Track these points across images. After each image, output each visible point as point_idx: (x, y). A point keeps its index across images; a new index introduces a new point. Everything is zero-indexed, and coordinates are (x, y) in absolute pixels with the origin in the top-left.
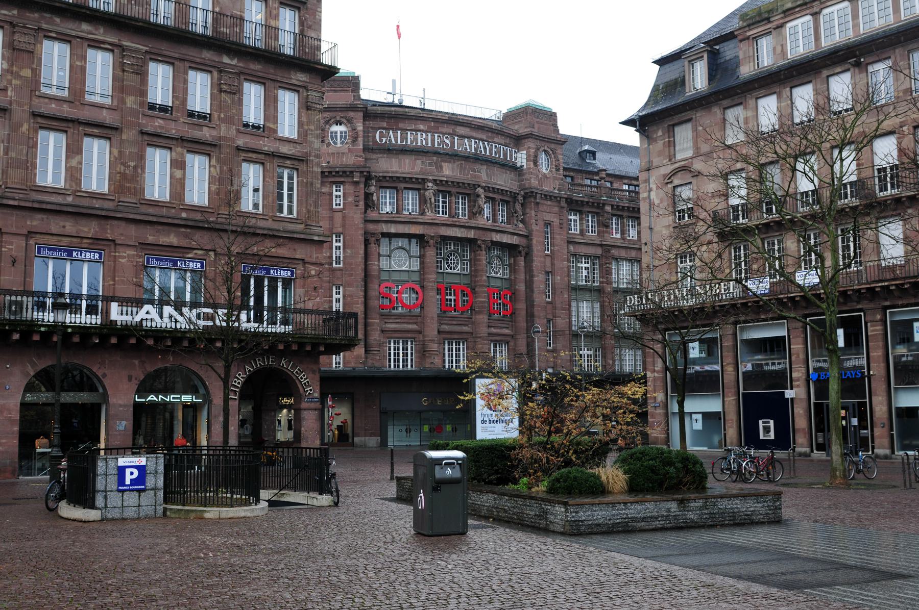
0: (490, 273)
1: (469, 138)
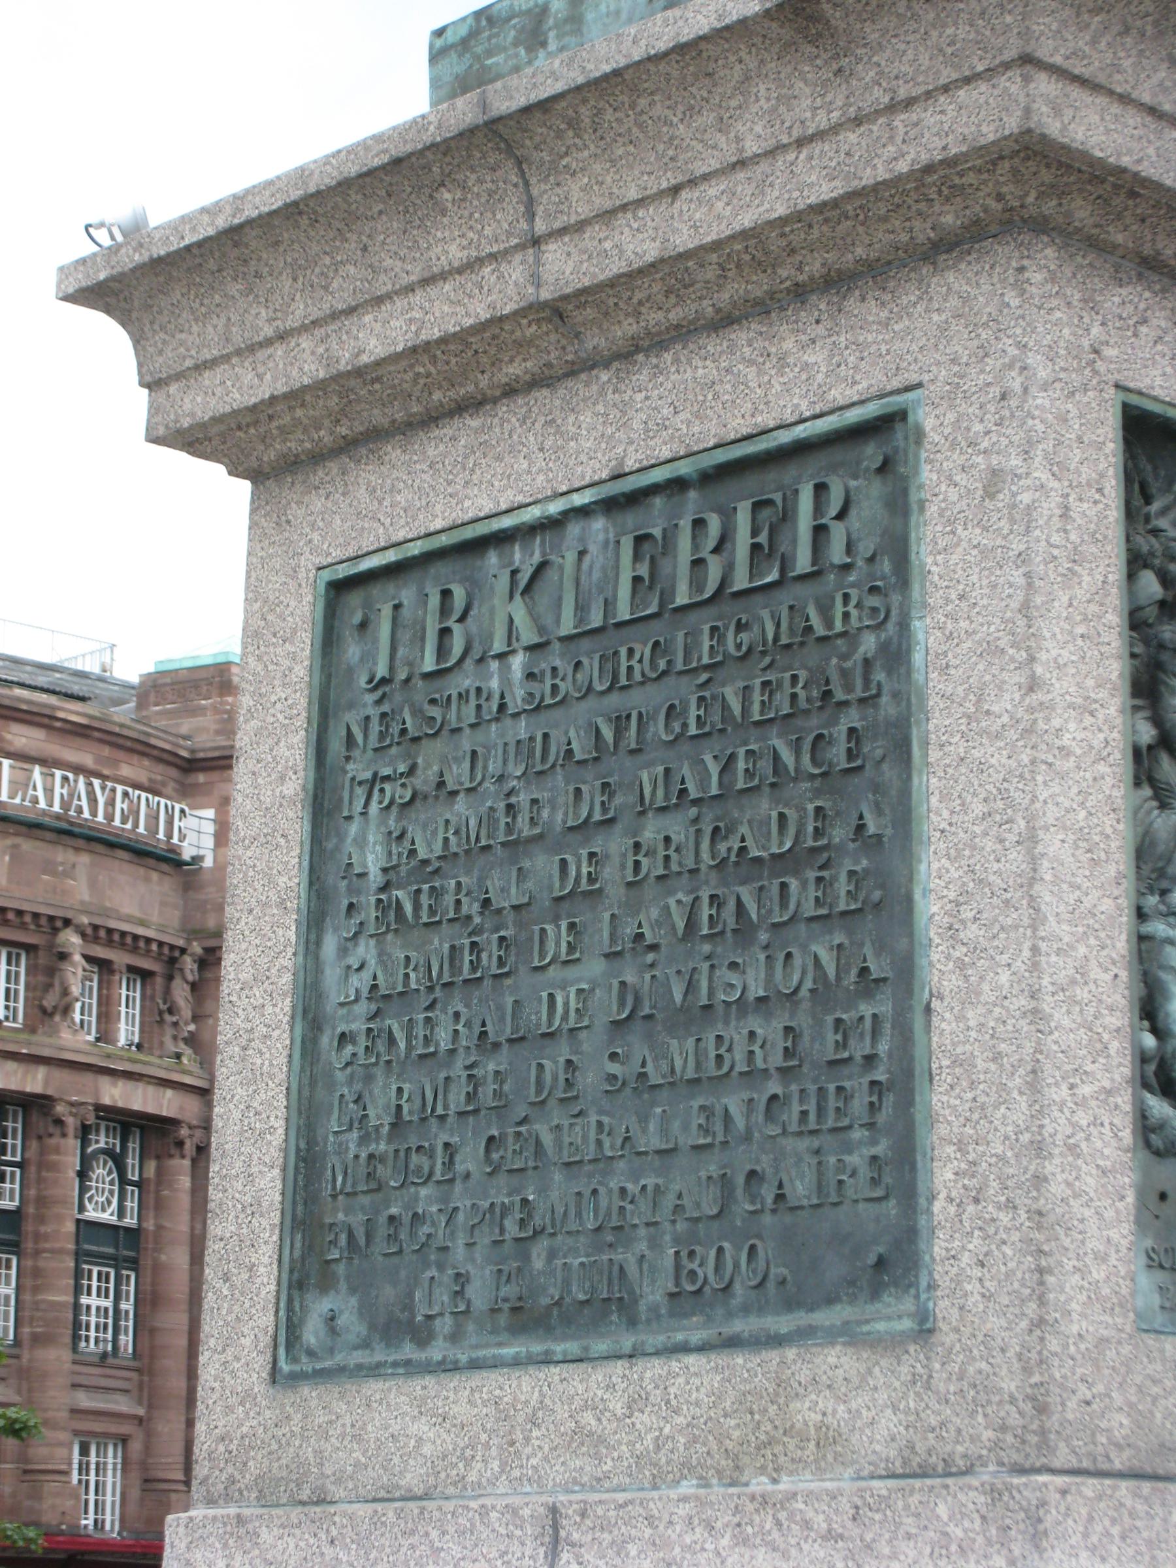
0: (82, 1208)
1: (43, 762)
